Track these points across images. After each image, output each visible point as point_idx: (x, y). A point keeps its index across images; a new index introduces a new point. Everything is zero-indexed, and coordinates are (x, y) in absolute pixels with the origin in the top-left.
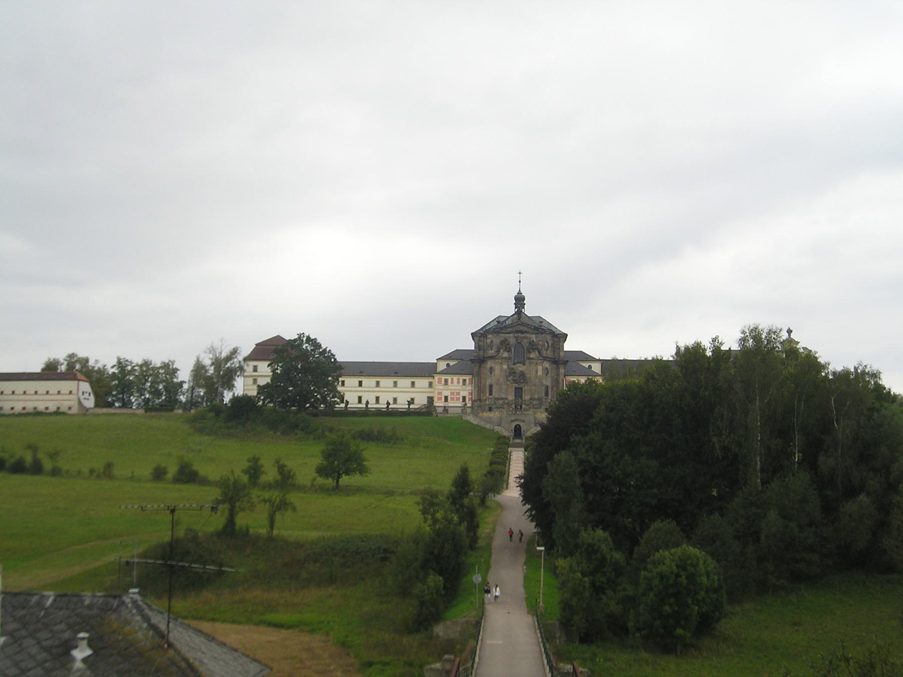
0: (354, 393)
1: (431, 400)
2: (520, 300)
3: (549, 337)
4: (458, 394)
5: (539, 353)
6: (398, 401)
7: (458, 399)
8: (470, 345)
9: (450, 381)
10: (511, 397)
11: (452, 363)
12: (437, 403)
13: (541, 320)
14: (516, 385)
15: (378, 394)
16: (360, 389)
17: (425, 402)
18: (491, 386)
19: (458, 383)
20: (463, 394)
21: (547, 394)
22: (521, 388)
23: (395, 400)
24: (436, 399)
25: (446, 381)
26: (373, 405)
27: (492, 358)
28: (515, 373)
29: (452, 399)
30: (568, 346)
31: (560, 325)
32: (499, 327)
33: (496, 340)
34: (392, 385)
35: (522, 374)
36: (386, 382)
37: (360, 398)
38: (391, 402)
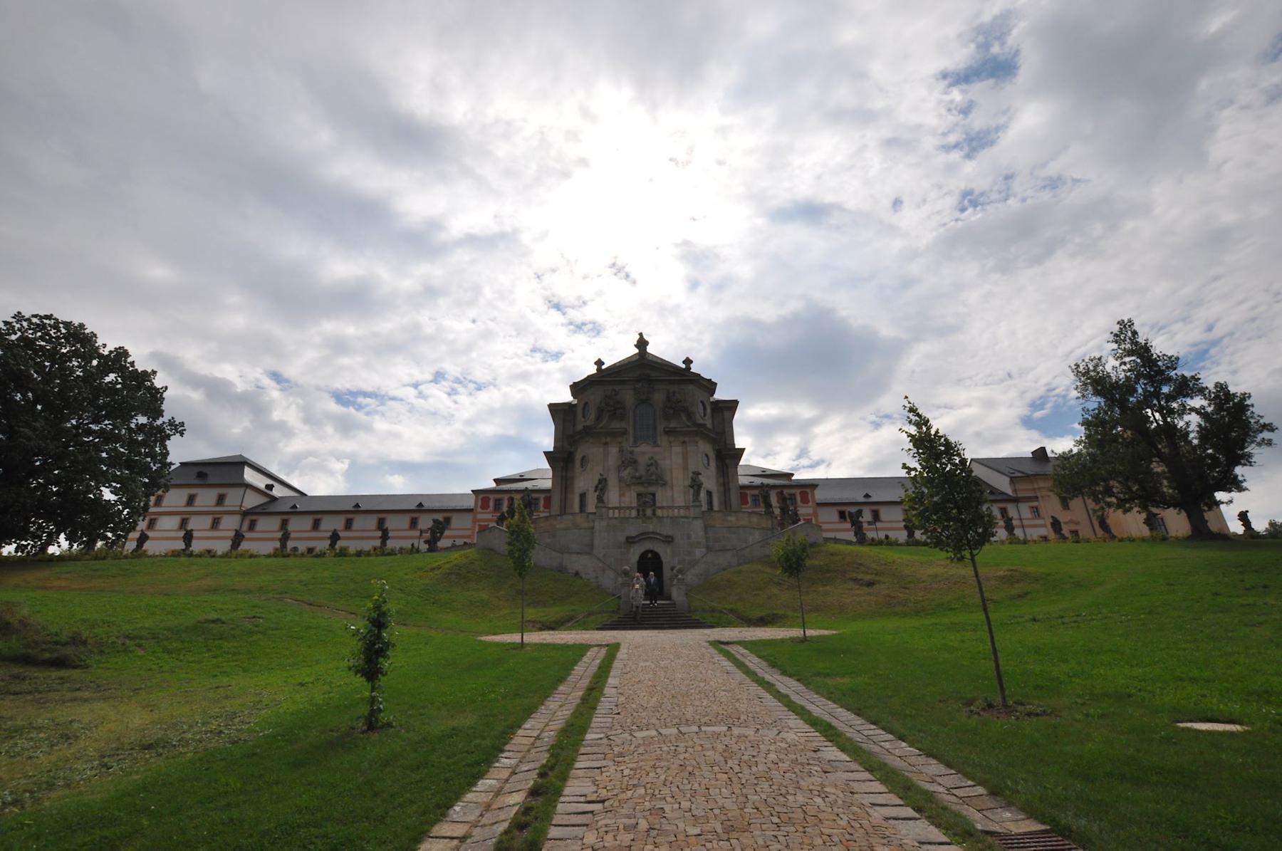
22: (654, 495)
28: (635, 462)
35: (653, 464)
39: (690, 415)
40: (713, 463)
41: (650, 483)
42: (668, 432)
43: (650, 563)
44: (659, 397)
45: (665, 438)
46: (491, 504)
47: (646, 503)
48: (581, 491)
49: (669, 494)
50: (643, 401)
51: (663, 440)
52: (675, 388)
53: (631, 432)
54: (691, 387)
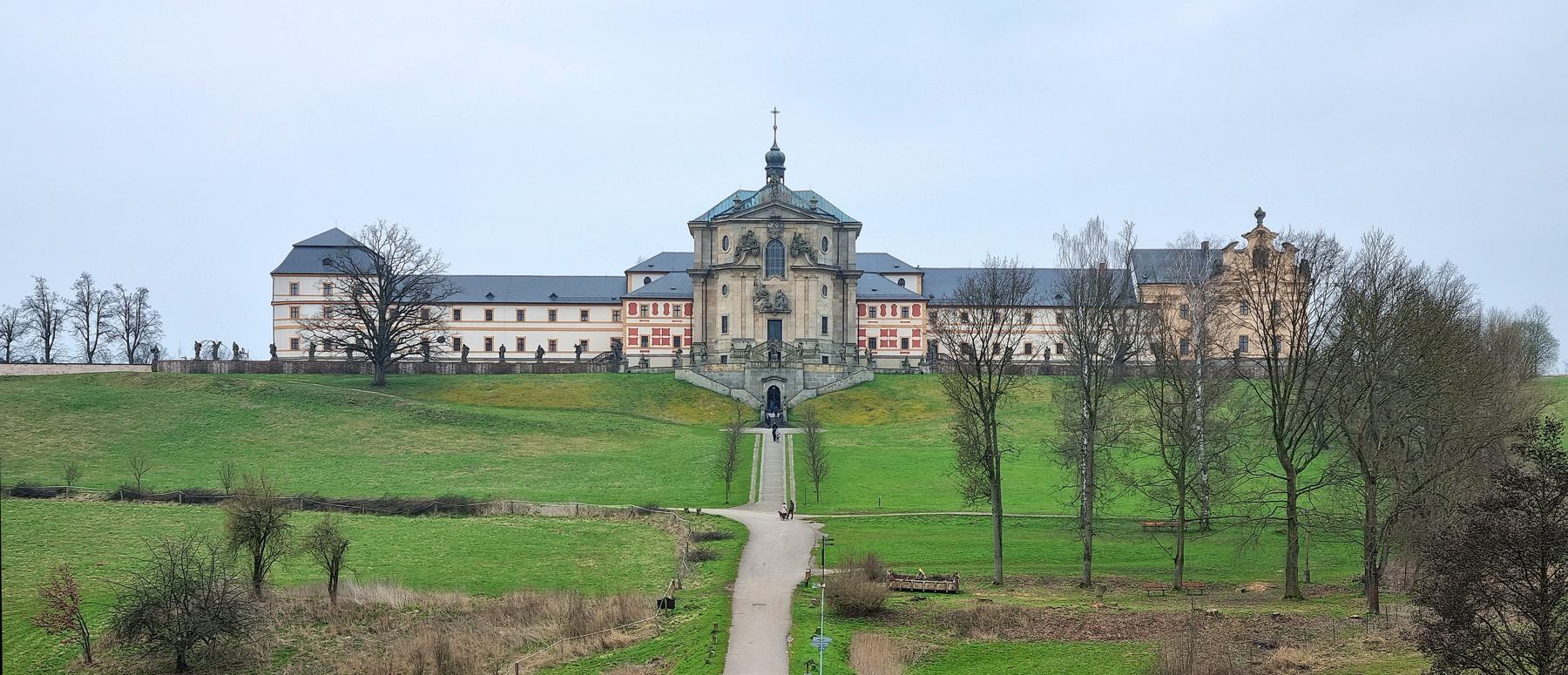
0: (475, 333)
1: (617, 344)
2: (775, 163)
3: (827, 232)
4: (666, 332)
5: (813, 258)
6: (559, 348)
7: (666, 342)
8: (686, 244)
10: (762, 338)
11: (653, 278)
12: (632, 351)
13: (815, 199)
14: (771, 317)
15: (521, 334)
16: (489, 325)
17: (607, 347)
18: (725, 319)
19: (666, 312)
20: (679, 332)
21: (825, 330)
23: (553, 344)
24: (626, 343)
25: (644, 308)
26: (512, 354)
27: (727, 268)
29: (656, 342)
30: (864, 244)
31: (849, 209)
32: (738, 209)
33: (734, 233)
35: (781, 296)
36: (537, 314)
37: (489, 345)
38: (546, 348)
39: (813, 258)
40: (830, 292)
41: (778, 312)
42: (795, 269)
43: (774, 394)
44: (787, 237)
47: (775, 328)
50: (775, 240)
51: (789, 275)
52: (801, 229)
54: (815, 227)
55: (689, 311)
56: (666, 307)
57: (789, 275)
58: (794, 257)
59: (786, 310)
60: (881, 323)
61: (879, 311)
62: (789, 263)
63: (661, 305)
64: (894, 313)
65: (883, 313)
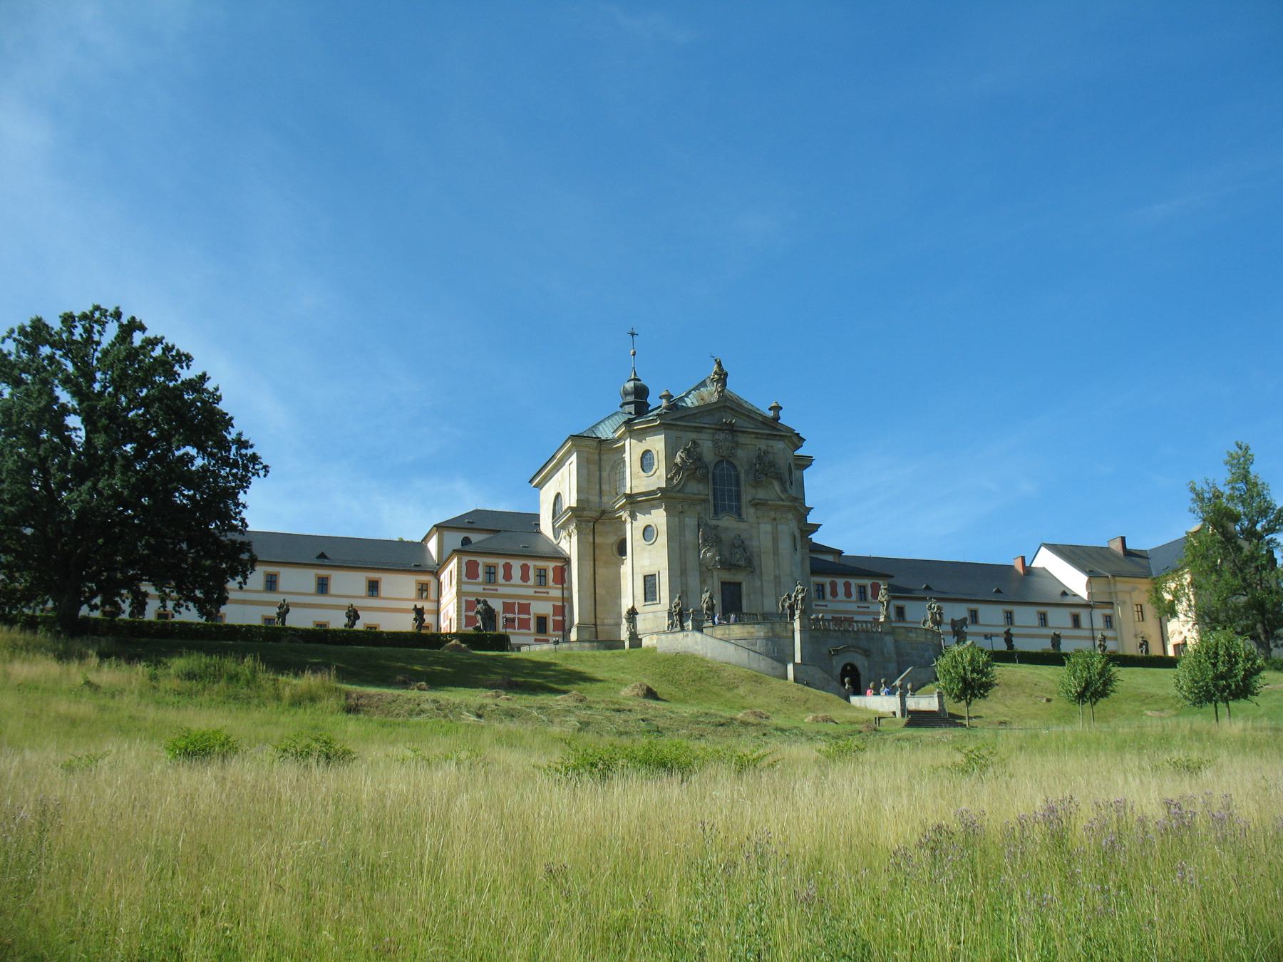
4: (525, 609)
9: (501, 572)
11: (475, 538)
14: (728, 576)
19: (525, 577)
20: (542, 608)
22: (740, 584)
25: (491, 572)
34: (312, 586)
35: (740, 545)
42: (757, 504)
45: (752, 511)
46: (481, 570)
48: (648, 571)
49: (758, 583)
50: (726, 462)
52: (763, 444)
53: (711, 498)
55: (562, 576)
56: (525, 569)
57: (748, 512)
58: (757, 484)
59: (750, 565)
60: (831, 606)
61: (828, 590)
62: (748, 493)
63: (516, 565)
64: (848, 594)
65: (834, 594)
